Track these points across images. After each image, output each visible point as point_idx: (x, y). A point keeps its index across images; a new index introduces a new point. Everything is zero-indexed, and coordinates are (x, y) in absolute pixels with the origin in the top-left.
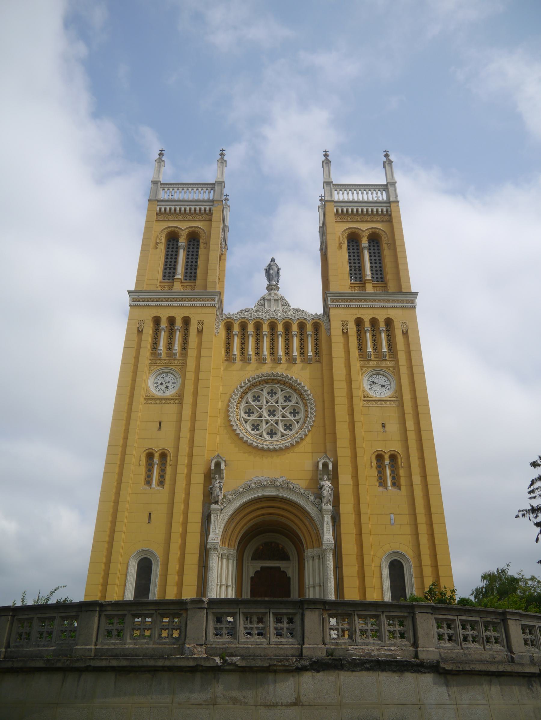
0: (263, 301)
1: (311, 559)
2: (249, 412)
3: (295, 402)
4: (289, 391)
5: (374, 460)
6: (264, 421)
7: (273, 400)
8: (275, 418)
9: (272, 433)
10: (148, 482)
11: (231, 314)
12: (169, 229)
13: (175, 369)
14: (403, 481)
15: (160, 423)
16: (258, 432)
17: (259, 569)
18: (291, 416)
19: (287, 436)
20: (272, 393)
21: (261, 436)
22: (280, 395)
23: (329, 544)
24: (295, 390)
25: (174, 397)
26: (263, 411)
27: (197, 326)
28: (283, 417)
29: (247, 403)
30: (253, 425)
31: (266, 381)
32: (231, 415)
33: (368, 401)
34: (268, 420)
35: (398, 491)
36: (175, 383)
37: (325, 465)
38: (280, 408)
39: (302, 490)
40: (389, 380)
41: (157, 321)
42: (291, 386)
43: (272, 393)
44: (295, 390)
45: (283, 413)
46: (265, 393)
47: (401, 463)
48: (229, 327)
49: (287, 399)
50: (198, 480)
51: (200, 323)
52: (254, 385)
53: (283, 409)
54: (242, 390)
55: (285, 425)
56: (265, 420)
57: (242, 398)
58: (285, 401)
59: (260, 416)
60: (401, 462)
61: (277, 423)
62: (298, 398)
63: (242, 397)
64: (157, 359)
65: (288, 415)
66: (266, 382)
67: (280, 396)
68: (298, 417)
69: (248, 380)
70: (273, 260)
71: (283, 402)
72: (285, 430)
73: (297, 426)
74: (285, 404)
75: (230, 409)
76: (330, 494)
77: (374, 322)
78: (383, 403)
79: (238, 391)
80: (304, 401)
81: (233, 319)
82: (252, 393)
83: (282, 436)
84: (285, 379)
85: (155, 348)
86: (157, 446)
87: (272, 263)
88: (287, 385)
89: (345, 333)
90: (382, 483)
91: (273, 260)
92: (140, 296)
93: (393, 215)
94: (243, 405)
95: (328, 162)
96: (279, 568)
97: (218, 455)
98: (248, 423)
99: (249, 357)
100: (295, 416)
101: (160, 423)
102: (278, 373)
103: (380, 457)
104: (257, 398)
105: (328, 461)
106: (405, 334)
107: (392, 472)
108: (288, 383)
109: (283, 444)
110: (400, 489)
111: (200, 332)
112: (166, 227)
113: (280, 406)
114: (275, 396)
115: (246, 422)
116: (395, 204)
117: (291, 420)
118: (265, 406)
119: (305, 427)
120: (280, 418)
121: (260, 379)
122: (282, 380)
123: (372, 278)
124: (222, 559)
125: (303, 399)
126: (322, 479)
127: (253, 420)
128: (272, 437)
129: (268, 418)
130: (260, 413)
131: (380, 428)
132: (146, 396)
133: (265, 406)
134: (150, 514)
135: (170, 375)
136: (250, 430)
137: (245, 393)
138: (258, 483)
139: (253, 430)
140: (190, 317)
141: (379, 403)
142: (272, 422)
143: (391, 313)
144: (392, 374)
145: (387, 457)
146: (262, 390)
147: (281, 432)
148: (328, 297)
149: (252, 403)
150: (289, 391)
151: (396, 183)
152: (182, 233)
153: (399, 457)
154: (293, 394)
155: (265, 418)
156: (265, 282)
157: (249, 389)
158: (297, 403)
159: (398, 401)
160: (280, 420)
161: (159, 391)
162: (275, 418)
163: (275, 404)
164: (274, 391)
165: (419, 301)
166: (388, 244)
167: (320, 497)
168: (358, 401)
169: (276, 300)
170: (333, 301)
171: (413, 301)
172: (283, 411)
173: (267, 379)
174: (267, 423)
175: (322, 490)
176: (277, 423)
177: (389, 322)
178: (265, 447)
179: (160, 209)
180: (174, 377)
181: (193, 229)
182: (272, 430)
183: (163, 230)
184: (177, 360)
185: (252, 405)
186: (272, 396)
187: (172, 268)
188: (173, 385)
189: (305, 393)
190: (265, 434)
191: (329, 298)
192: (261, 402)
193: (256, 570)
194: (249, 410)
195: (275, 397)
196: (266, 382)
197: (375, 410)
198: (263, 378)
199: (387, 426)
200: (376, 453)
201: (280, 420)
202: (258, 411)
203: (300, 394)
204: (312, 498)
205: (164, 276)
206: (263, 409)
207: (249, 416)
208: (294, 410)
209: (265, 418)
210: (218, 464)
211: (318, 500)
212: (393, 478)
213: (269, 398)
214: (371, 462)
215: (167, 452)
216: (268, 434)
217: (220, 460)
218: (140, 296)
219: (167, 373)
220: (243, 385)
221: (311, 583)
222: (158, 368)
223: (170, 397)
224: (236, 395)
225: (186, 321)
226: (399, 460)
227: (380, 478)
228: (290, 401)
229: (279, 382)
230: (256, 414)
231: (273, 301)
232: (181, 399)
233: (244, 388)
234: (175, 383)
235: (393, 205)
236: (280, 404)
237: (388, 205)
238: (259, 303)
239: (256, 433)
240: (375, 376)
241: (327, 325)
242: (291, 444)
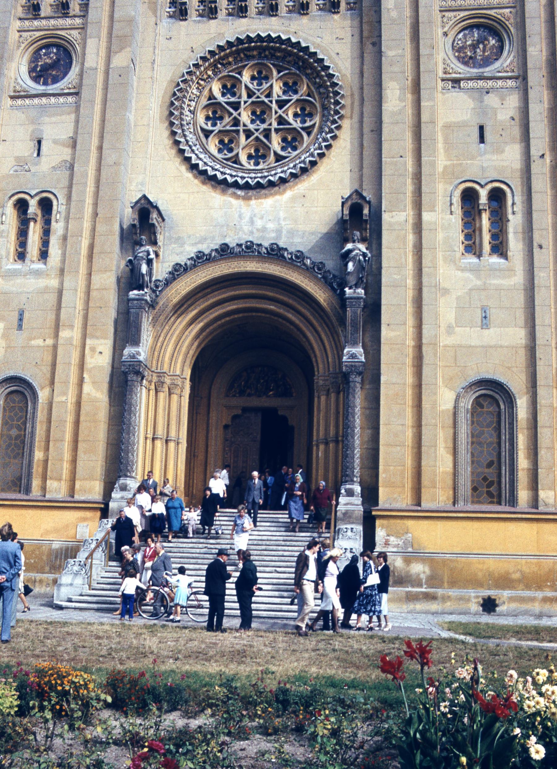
1: (325, 392)
3: (305, 92)
6: (241, 131)
7: (261, 91)
8: (265, 126)
10: (21, 256)
16: (230, 155)
17: (240, 412)
18: (296, 121)
21: (235, 162)
26: (239, 114)
29: (210, 99)
32: (174, 121)
34: (249, 130)
38: (274, 106)
45: (280, 116)
46: (246, 77)
47: (513, 204)
49: (289, 88)
53: (280, 107)
56: (244, 131)
58: (284, 92)
59: (236, 122)
62: (310, 84)
65: (290, 119)
71: (281, 93)
72: (283, 149)
74: (284, 98)
75: (174, 109)
80: (322, 90)
83: (277, 161)
88: (289, 59)
98: (210, 139)
99: (213, 6)
107: (493, 223)
113: (274, 102)
114: (266, 83)
115: (207, 137)
117: (295, 129)
118: (245, 102)
119: (320, 140)
120: (275, 125)
124: (157, 392)
127: (220, 131)
128: (257, 164)
129: (252, 127)
130: (235, 118)
133: (245, 102)
139: (220, 151)
142: (256, 134)
146: (240, 73)
147: (275, 153)
155: (245, 125)
158: (309, 95)
160: (273, 130)
162: (265, 126)
164: (264, 73)
172: (280, 112)
174: (248, 137)
178: (241, 182)
185: (219, 104)
186: (260, 84)
190: (243, 158)
192: (238, 95)
193: (233, 414)
195: (265, 86)
201: (273, 130)
202: (230, 114)
206: (242, 110)
207: (214, 125)
212: (494, 236)
213: (253, 86)
214: (451, 204)
215: (51, 196)
227: (468, 237)
228: (296, 92)
230: (227, 119)
236: (275, 97)
239: (226, 157)
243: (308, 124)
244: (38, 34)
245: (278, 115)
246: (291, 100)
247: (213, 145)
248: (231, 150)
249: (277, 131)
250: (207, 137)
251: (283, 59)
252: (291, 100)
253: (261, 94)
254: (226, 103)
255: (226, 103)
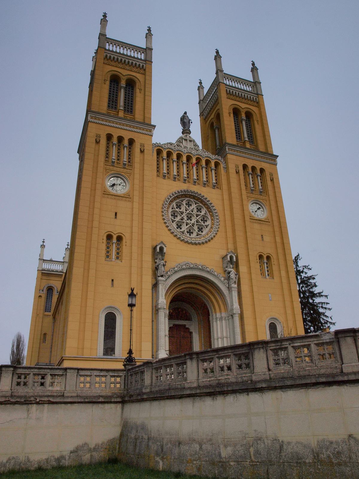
0: (180, 140)
2: (174, 215)
4: (201, 205)
5: (258, 258)
6: (185, 223)
9: (190, 232)
11: (161, 144)
12: (113, 72)
13: (124, 175)
14: (276, 273)
15: (116, 214)
19: (201, 236)
20: (189, 205)
21: (183, 233)
22: (194, 206)
23: (237, 310)
24: (205, 204)
25: (126, 196)
27: (140, 147)
28: (197, 222)
29: (172, 209)
30: (177, 225)
31: (186, 195)
33: (252, 219)
35: (273, 280)
36: (124, 186)
37: (231, 257)
39: (216, 273)
40: (263, 209)
41: (109, 137)
42: (202, 202)
43: (189, 205)
44: (205, 204)
46: (184, 203)
48: (159, 152)
49: (199, 210)
50: (148, 257)
51: (142, 145)
52: (177, 197)
54: (171, 199)
55: (198, 228)
57: (170, 205)
58: (197, 211)
60: (274, 261)
61: (193, 226)
63: (170, 204)
64: (111, 166)
66: (185, 196)
67: (195, 207)
68: (206, 224)
69: (175, 193)
70: (185, 113)
73: (205, 231)
76: (236, 278)
77: (253, 168)
78: (261, 222)
79: (168, 199)
81: (162, 147)
82: (176, 202)
83: (197, 235)
84: (199, 196)
85: (107, 157)
86: (116, 231)
87: (185, 115)
89: (237, 172)
90: (262, 274)
91: (185, 113)
92: (97, 116)
93: (261, 103)
94: (170, 210)
95: (220, 57)
96: (185, 326)
97: (162, 243)
100: (204, 223)
101: (116, 214)
102: (194, 191)
103: (261, 257)
104: (179, 206)
105: (233, 255)
106: (272, 180)
108: (200, 199)
109: (200, 240)
110: (273, 278)
111: (142, 152)
112: (111, 70)
115: (173, 222)
116: (262, 96)
120: (196, 223)
121: (182, 193)
122: (196, 197)
123: (249, 139)
125: (209, 212)
126: (227, 267)
128: (190, 235)
129: (188, 221)
131: (260, 238)
132: (104, 192)
134: (113, 280)
135: (120, 179)
136: (176, 228)
137: (172, 201)
138: (187, 266)
139: (177, 228)
140: (135, 140)
141: (259, 222)
143: (264, 165)
144: (265, 204)
145: (265, 257)
146: (182, 202)
148: (226, 146)
149: (177, 210)
150: (201, 205)
151: (261, 83)
152: (122, 77)
153: (272, 258)
154: (203, 207)
156: (180, 128)
157: (175, 199)
159: (270, 222)
161: (112, 189)
163: (191, 212)
165: (278, 160)
166: (257, 121)
167: (229, 278)
168: (247, 218)
169: (190, 141)
170: (229, 149)
171: (275, 161)
173: (187, 194)
175: (230, 274)
176: (193, 226)
177: (262, 170)
179: (106, 56)
180: (123, 181)
181: (131, 77)
182: (190, 230)
183: (109, 72)
184: (126, 169)
187: (114, 102)
188: (122, 187)
189: (212, 208)
191: (227, 147)
194: (174, 214)
196: (185, 196)
197: (256, 226)
198: (184, 193)
199: (264, 237)
200: (259, 254)
203: (208, 208)
204: (222, 279)
205: (109, 106)
208: (204, 218)
209: (186, 221)
210: (161, 249)
211: (226, 281)
216: (188, 232)
217: (163, 246)
218: (97, 116)
219: (118, 177)
220: (172, 195)
221: (219, 335)
222: (112, 172)
223: (122, 195)
224: (167, 201)
225: (131, 142)
226: (272, 260)
229: (194, 197)
231: (188, 141)
232: (130, 198)
233: (172, 198)
234: (124, 186)
235: (260, 96)
237: (257, 96)
238: (178, 140)
240: (254, 204)
241: (224, 165)
242: (206, 241)
243: (206, 224)
244: (113, 172)
245: (197, 219)
246: (201, 215)
247: (174, 225)
248: (181, 229)
249: (197, 225)
250: (173, 222)
251: (197, 200)
252: (201, 215)
253: (191, 210)
254: (179, 211)
255: (179, 211)
